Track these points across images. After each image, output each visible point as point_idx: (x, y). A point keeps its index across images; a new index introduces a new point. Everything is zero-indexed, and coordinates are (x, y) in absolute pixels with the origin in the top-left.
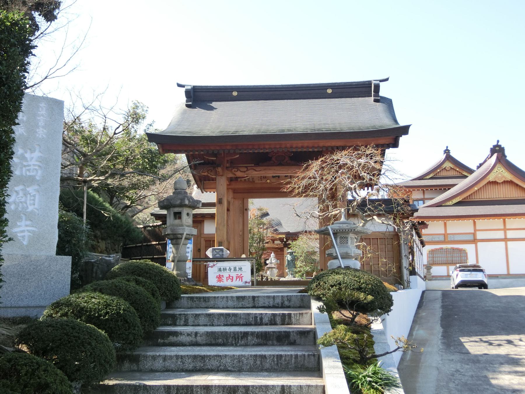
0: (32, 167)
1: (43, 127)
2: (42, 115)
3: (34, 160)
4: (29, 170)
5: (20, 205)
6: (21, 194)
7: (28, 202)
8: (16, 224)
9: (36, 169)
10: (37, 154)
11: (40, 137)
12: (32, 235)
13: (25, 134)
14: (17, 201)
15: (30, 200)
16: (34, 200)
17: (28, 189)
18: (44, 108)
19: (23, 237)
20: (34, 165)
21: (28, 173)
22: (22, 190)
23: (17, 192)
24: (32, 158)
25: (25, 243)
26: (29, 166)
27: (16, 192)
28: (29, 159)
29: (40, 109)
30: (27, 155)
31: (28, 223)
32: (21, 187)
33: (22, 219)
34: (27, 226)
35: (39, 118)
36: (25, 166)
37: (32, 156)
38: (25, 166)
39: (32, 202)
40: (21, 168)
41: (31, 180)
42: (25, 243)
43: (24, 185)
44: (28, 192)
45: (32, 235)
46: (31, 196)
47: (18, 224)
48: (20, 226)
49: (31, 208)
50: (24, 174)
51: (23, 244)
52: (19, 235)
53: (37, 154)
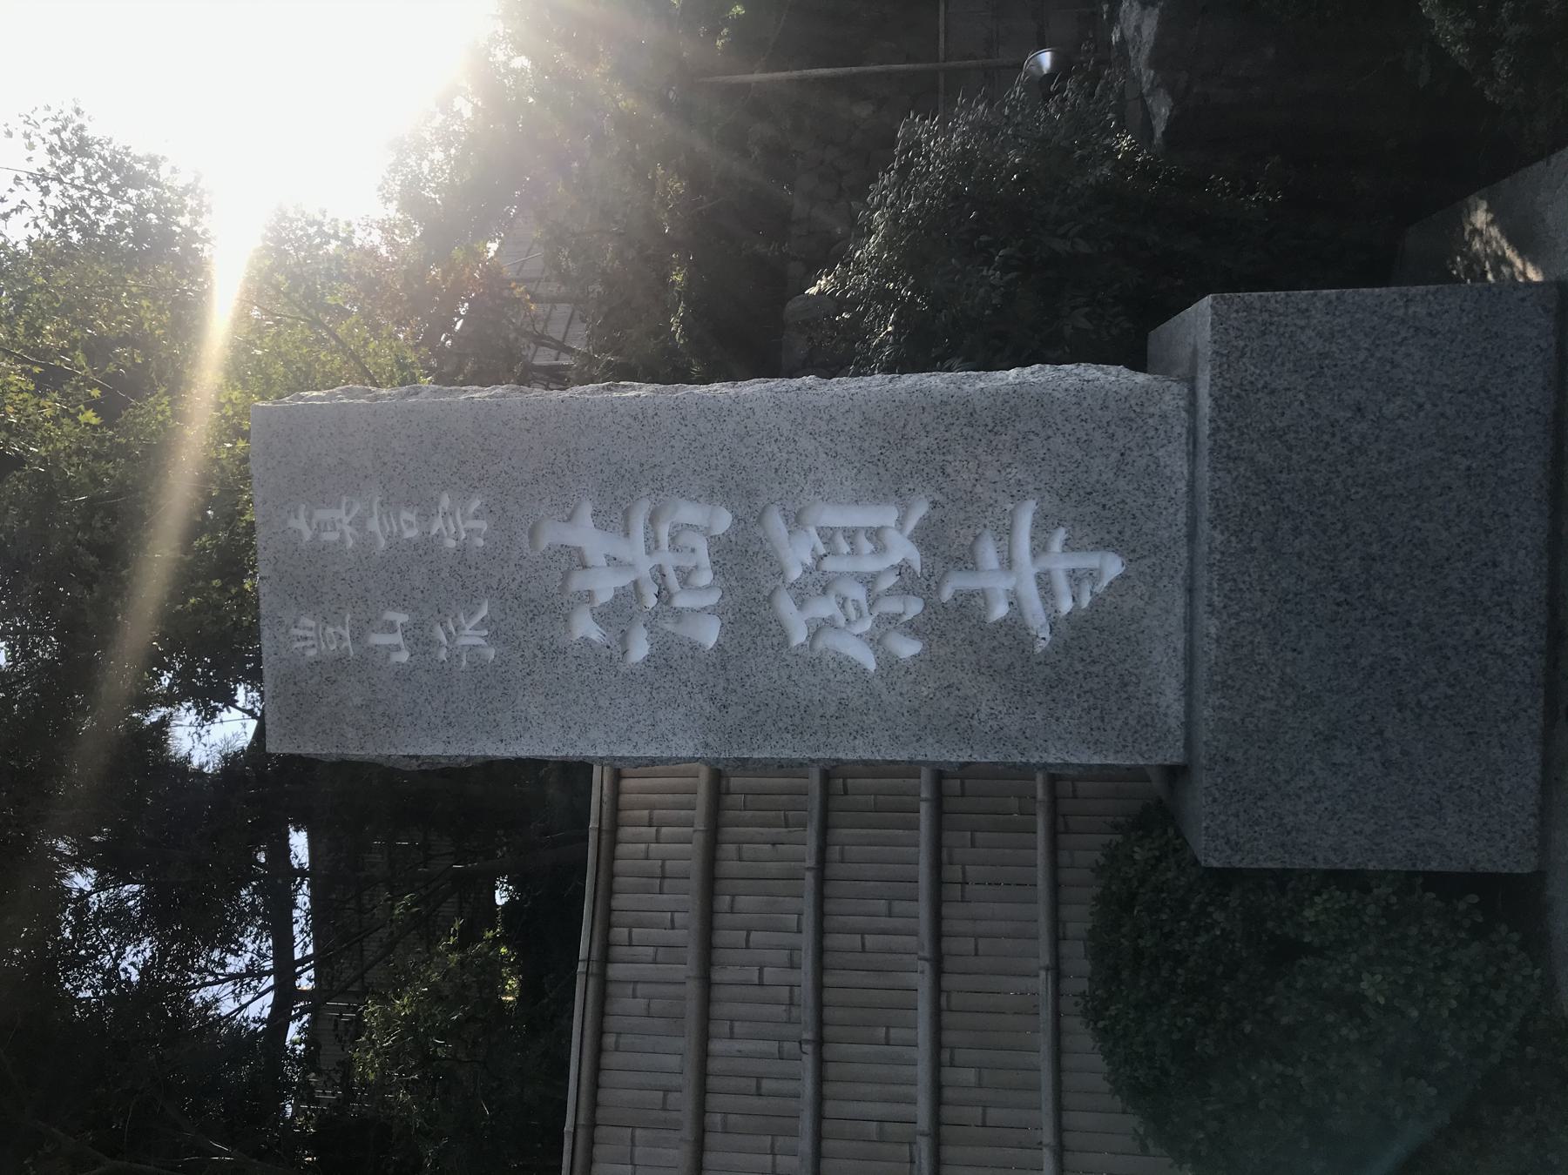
0: (668, 560)
1: (426, 516)
2: (360, 523)
3: (621, 549)
4: (685, 577)
5: (892, 606)
6: (825, 608)
7: (869, 565)
8: (1001, 623)
9: (673, 539)
10: (585, 535)
11: (482, 525)
12: (1061, 534)
13: (484, 612)
14: (866, 625)
15: (854, 552)
16: (851, 534)
17: (795, 573)
18: (322, 515)
19: (1074, 577)
20: (652, 546)
21: (705, 578)
22: (801, 603)
23: (818, 628)
24: (613, 561)
25: (1112, 566)
26: (659, 573)
27: (813, 636)
28: (624, 580)
29: (332, 537)
30: (605, 586)
31: (989, 554)
32: (786, 605)
33: (972, 595)
34: (1008, 563)
35: (383, 543)
36: (664, 595)
37: (603, 562)
38: (664, 595)
39: (866, 546)
40: (679, 614)
41: (742, 559)
42: (1112, 566)
43: (769, 599)
44: (807, 571)
45: (1061, 534)
46: (833, 552)
47: (1000, 611)
48: (1015, 602)
49: (903, 550)
50: (713, 598)
51: (1123, 577)
52: (1066, 606)
53: (585, 535)
